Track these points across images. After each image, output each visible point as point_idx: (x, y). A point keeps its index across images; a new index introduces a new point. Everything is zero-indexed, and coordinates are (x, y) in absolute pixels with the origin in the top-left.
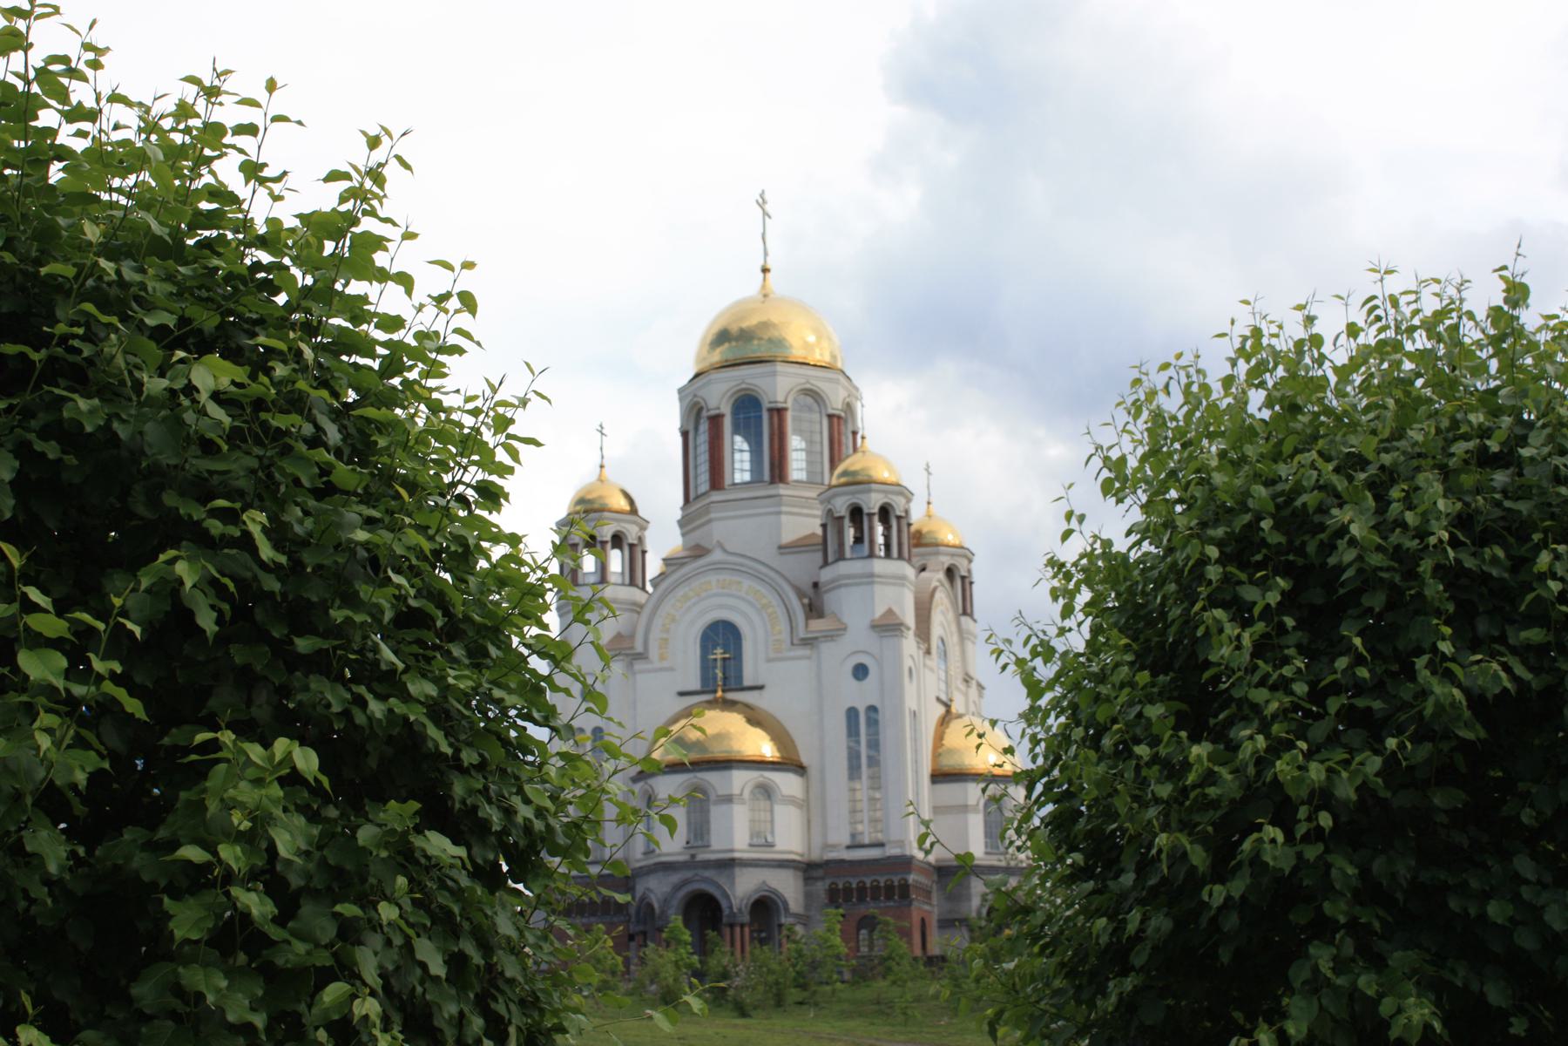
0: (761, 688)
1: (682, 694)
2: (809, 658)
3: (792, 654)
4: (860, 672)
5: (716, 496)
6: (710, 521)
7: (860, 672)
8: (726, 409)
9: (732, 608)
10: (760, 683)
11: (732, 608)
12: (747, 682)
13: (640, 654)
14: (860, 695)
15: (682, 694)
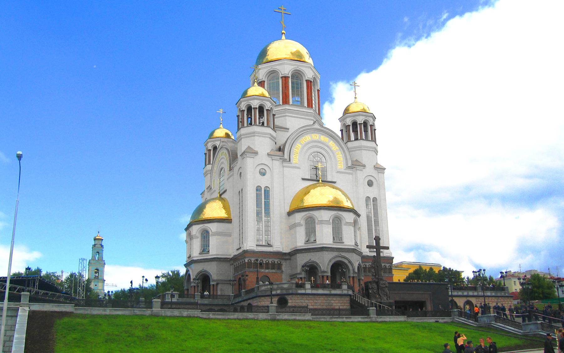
0: (335, 182)
1: (303, 179)
2: (352, 174)
3: (347, 171)
4: (370, 184)
5: (287, 107)
6: (286, 116)
7: (370, 184)
8: (290, 75)
9: (321, 148)
10: (334, 180)
11: (321, 148)
12: (329, 179)
13: (286, 159)
14: (372, 192)
15: (303, 179)
